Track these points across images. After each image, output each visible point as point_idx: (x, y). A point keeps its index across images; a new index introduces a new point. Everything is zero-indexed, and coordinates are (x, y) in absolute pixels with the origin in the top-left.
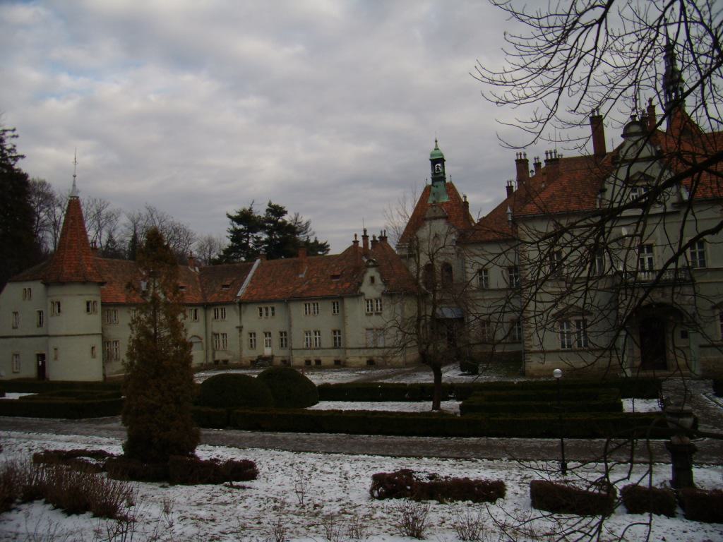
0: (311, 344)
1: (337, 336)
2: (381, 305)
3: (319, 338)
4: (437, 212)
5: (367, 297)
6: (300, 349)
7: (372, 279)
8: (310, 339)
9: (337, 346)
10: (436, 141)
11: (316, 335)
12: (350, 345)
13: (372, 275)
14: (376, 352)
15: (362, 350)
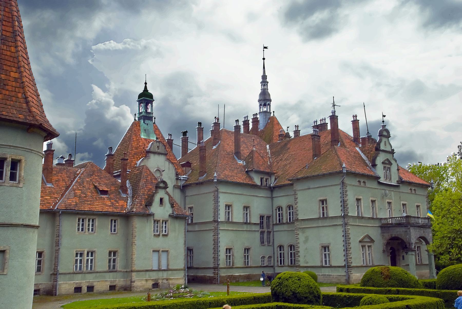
0: (81, 266)
1: (112, 257)
2: (165, 227)
3: (92, 260)
4: (160, 147)
5: (156, 218)
6: (69, 274)
7: (161, 200)
8: (81, 260)
9: (112, 269)
10: (146, 83)
11: (88, 256)
12: (135, 268)
13: (162, 197)
14: (161, 275)
15: (148, 273)
